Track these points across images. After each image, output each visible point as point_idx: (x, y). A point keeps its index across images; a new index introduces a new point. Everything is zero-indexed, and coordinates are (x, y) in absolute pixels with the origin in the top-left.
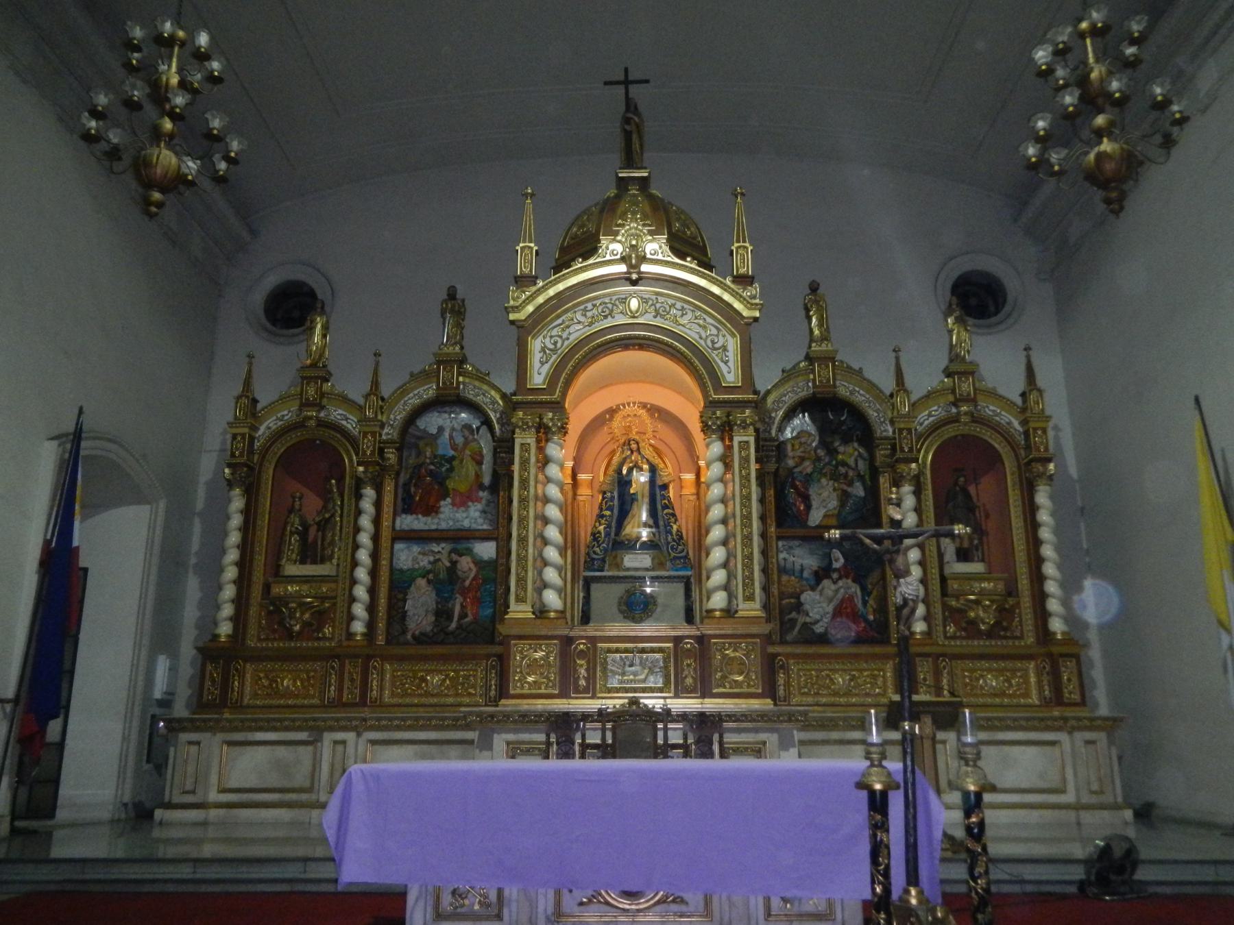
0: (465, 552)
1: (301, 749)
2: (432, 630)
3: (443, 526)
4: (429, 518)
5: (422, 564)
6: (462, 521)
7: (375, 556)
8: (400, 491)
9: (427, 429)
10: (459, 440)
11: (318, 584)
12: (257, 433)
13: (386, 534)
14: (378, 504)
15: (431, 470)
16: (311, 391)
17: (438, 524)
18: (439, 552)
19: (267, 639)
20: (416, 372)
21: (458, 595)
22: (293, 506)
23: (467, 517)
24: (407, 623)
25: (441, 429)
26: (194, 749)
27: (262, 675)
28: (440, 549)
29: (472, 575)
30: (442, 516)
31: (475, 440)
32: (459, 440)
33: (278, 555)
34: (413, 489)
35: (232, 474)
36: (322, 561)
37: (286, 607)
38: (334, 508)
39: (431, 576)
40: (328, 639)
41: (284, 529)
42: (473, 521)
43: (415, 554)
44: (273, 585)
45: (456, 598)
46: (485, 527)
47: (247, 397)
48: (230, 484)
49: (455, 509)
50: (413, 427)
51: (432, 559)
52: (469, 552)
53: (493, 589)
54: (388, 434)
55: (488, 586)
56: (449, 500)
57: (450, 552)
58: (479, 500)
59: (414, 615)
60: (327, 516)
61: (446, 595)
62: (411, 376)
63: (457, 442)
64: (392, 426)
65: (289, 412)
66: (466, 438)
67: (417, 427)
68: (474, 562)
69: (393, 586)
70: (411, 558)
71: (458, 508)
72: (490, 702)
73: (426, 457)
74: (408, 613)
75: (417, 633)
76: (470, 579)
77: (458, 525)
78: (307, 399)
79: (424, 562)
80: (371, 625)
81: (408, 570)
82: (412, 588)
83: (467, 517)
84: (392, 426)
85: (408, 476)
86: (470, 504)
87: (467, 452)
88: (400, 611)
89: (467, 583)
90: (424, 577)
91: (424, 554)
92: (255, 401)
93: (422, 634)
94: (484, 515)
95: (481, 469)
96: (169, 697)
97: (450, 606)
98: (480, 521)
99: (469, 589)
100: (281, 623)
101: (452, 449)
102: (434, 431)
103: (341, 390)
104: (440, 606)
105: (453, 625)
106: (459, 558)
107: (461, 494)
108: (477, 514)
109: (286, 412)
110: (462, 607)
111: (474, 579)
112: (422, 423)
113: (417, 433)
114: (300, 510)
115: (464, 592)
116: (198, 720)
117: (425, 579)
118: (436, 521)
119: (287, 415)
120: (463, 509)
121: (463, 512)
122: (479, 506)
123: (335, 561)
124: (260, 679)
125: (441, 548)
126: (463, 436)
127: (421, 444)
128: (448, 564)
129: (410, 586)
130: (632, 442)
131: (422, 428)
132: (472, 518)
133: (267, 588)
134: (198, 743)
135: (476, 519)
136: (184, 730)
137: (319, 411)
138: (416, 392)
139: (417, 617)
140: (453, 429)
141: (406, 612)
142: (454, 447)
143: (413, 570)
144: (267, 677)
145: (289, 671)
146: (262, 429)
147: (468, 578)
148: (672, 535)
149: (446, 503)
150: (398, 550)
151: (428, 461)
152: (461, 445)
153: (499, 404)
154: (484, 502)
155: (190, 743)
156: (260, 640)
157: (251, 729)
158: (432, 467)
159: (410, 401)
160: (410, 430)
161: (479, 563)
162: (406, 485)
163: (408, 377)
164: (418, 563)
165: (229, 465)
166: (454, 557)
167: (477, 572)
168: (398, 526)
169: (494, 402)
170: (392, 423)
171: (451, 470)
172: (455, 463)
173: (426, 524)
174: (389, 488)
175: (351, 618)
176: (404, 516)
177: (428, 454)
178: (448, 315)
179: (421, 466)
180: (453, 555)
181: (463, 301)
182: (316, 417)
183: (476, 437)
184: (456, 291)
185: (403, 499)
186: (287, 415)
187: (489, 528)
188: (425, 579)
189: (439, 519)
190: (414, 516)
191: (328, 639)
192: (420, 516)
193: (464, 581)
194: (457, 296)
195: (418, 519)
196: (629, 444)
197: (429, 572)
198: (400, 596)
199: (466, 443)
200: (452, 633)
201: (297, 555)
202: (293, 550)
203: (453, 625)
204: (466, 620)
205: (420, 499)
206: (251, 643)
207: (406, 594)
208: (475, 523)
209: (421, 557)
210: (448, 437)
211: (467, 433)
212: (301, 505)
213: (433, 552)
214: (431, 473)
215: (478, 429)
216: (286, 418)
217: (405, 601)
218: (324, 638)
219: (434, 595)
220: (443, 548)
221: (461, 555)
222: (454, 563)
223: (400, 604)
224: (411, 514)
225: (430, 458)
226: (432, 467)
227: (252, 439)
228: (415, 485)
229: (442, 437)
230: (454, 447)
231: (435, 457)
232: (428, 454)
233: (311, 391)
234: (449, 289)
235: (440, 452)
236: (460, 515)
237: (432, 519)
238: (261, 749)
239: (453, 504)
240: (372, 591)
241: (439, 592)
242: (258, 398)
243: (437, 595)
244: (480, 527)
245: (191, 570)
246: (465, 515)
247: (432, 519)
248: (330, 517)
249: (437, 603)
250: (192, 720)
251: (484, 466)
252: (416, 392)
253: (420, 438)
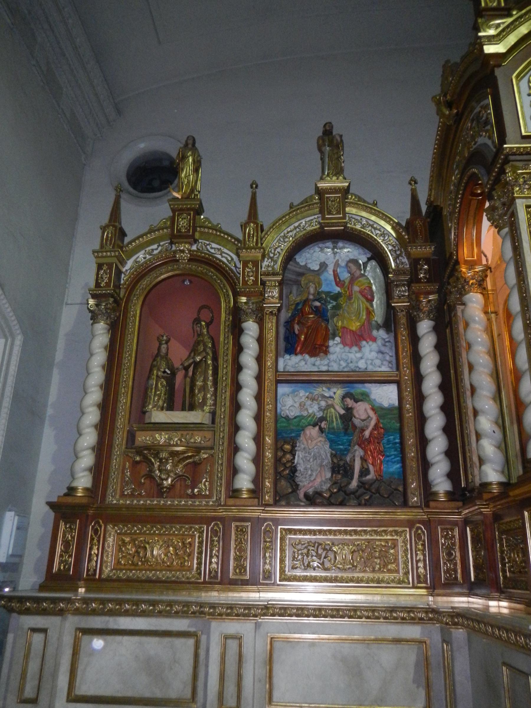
0: (361, 398)
1: (179, 642)
2: (329, 490)
3: (335, 367)
4: (318, 359)
5: (310, 411)
6: (357, 362)
7: (259, 398)
8: (282, 330)
9: (309, 266)
10: (345, 276)
11: (190, 432)
12: (124, 267)
13: (269, 375)
14: (260, 340)
15: (316, 307)
16: (183, 223)
17: (328, 365)
18: (331, 397)
19: (132, 496)
20: (295, 204)
21: (357, 447)
22: (159, 349)
23: (362, 358)
24: (297, 480)
25: (323, 266)
26: (38, 638)
27: (127, 539)
28: (332, 394)
29: (373, 423)
30: (332, 357)
31: (363, 275)
32: (345, 276)
33: (144, 401)
34: (297, 327)
35: (97, 305)
36: (192, 408)
37: (156, 456)
38: (204, 350)
39: (323, 425)
40: (206, 496)
41: (151, 370)
42: (369, 362)
43: (303, 400)
44: (138, 433)
45: (355, 451)
46: (384, 368)
47: (114, 226)
48: (94, 317)
49: (347, 348)
50: (291, 263)
51: (323, 404)
52: (365, 397)
53: (397, 441)
54: (268, 266)
55: (392, 437)
56: (338, 339)
57: (344, 397)
58: (374, 340)
59: (306, 469)
60: (198, 359)
61: (341, 447)
62: (291, 208)
63: (342, 279)
64: (272, 258)
65: (158, 246)
66: (352, 275)
67: (298, 263)
68: (373, 409)
69: (278, 436)
70: (297, 405)
71: (350, 348)
72: (419, 582)
73: (309, 293)
74: (299, 468)
75: (311, 491)
76: (370, 428)
77: (352, 366)
78: (179, 231)
79: (314, 409)
80: (257, 480)
81: (295, 418)
82: (302, 438)
83: (362, 358)
84: (272, 258)
85: (290, 315)
86: (364, 343)
87: (356, 288)
88: (288, 465)
89: (367, 433)
90: (314, 425)
91: (313, 399)
92: (123, 234)
93: (318, 494)
94: (380, 355)
95: (372, 306)
96: (16, 560)
97: (348, 459)
98: (378, 362)
99: (369, 441)
100: (150, 476)
101: (337, 284)
102: (315, 267)
103: (215, 224)
104: (335, 461)
105: (354, 484)
106: (355, 404)
107: (353, 333)
108: (374, 354)
109: (155, 246)
110: (363, 459)
111: (376, 427)
112: (302, 259)
113: (297, 270)
114: (167, 354)
115: (363, 443)
116: (45, 599)
117: (317, 428)
118: (326, 362)
119: (157, 249)
120: (355, 349)
121: (356, 352)
122: (374, 346)
123: (207, 409)
124: (124, 543)
125: (339, 392)
126: (349, 272)
127: (303, 281)
128: (342, 412)
129: (299, 436)
131: (302, 264)
132: (367, 359)
133: (131, 437)
134: (44, 631)
135: (372, 360)
136: (28, 612)
137: (191, 245)
138: (296, 224)
139: (309, 472)
140: (337, 264)
141: (295, 467)
142: (339, 282)
143: (300, 418)
144: (133, 541)
145: (160, 535)
146: (130, 263)
147: (367, 427)
149: (335, 342)
150: (284, 395)
151: (311, 297)
152: (347, 282)
153: (389, 234)
154: (379, 342)
155: (34, 630)
156: (122, 495)
157: (112, 613)
158: (317, 304)
159: (290, 234)
160: (289, 266)
161: (378, 409)
162: (289, 324)
163: (287, 210)
164: (307, 409)
165: (94, 296)
166: (350, 402)
167: (378, 421)
168: (281, 367)
169: (384, 234)
170: (272, 255)
171: (337, 307)
172: (341, 300)
173: (314, 365)
174: (270, 324)
175: (234, 471)
176: (287, 357)
177: (312, 290)
178: (328, 148)
179: (306, 302)
180: (348, 400)
181: (341, 136)
182: (190, 251)
183: (362, 272)
184: (332, 127)
185: (286, 339)
186: (157, 249)
187: (388, 369)
188: (317, 428)
189: (328, 359)
190: (299, 357)
191: (206, 496)
192: (307, 357)
193: (363, 430)
194: (334, 133)
195: (304, 360)
197: (322, 419)
198: (287, 447)
199: (353, 279)
200: (354, 493)
201: (164, 403)
202: (159, 396)
203: (354, 484)
204: (369, 477)
205: (305, 338)
206: (113, 499)
207: (294, 446)
208: (371, 364)
209: (309, 402)
210: (332, 273)
211: (353, 267)
212: (168, 349)
213: (324, 397)
214: (317, 311)
215: (365, 264)
216: (155, 252)
217: (293, 452)
218: (200, 496)
219: (327, 446)
220: (335, 393)
221: (356, 401)
222: (349, 410)
223: (289, 456)
224: (296, 354)
225: (313, 295)
226: (317, 304)
227: (119, 273)
228: (298, 324)
229: (325, 274)
230: (339, 282)
231: (319, 293)
232: (312, 290)
233: (183, 223)
234: (325, 126)
235: (324, 288)
236: (353, 354)
237: (321, 360)
238: (126, 639)
239: (344, 343)
240: (258, 439)
241: (332, 442)
242: (127, 230)
243: (331, 447)
245: (47, 422)
246: (359, 355)
247: (321, 360)
248: (201, 360)
249: (333, 456)
250: (37, 600)
251: (374, 303)
252: (296, 224)
253: (302, 274)
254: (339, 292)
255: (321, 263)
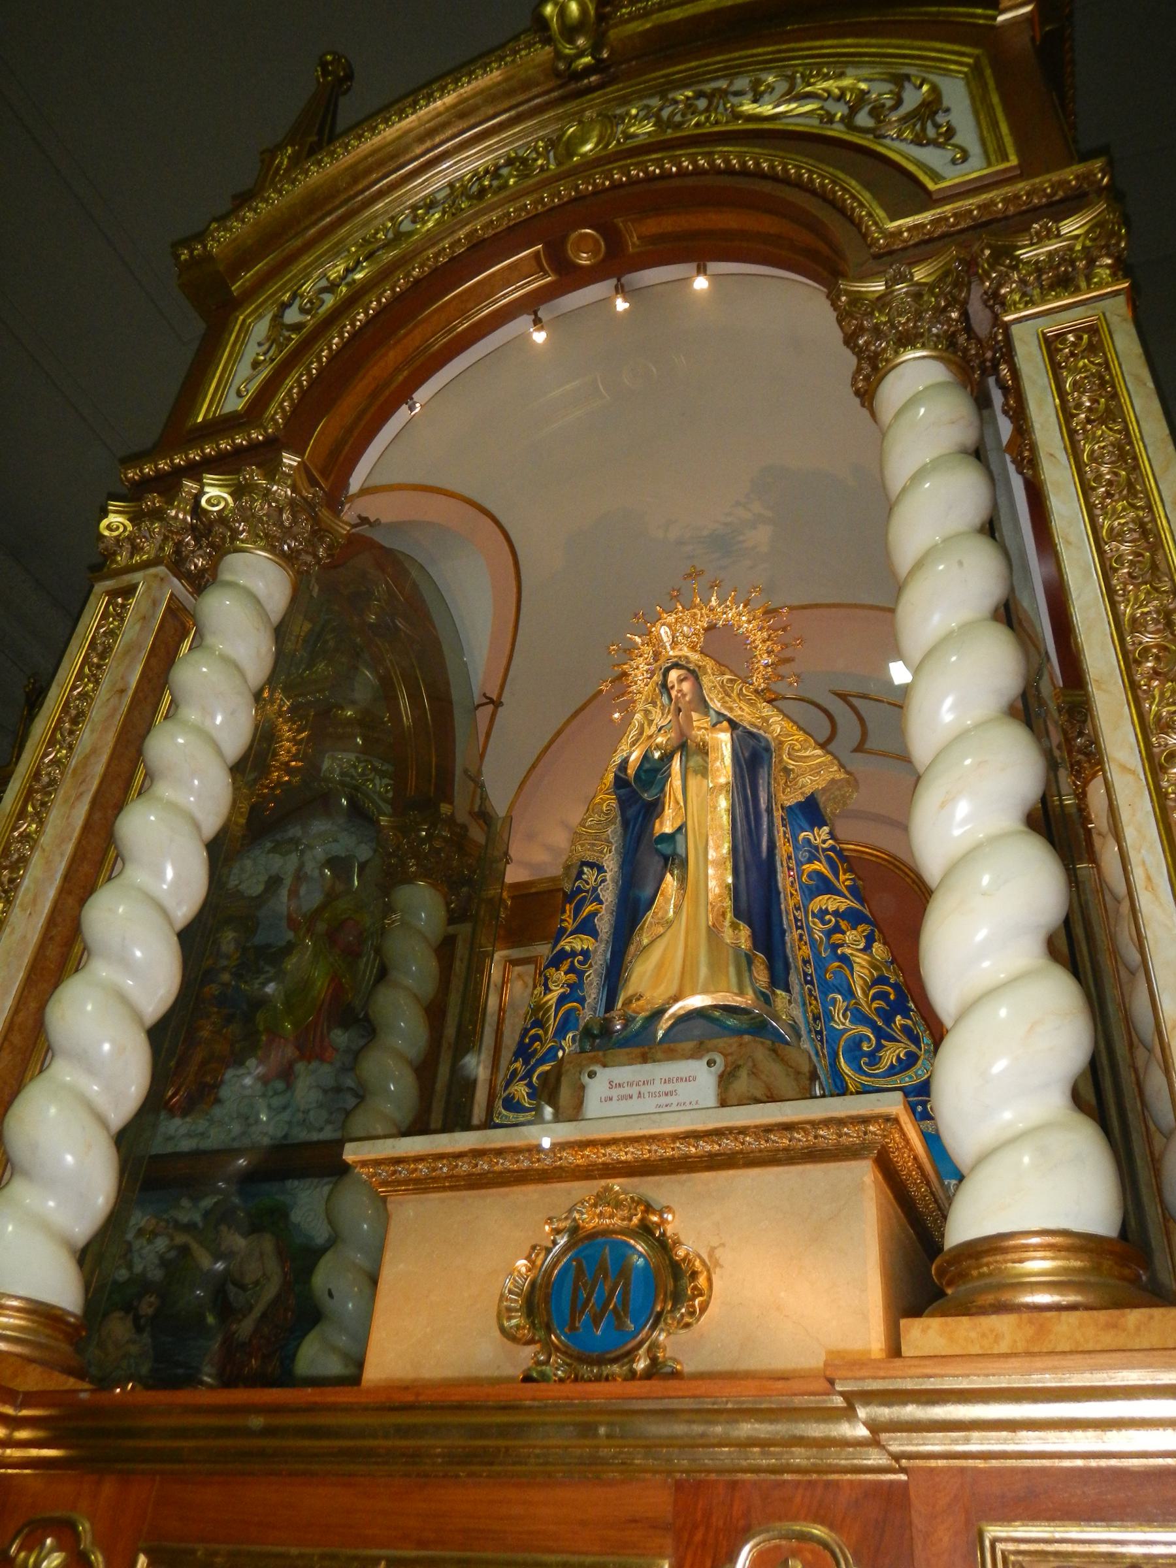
5: (138, 1268)
18: (189, 1228)
23: (285, 1108)
28: (197, 1218)
76: (257, 1313)
130: (674, 675)
148: (849, 993)
164: (130, 1266)
196: (665, 687)
244: (315, 1136)
254: (289, 942)
255: (270, 877)
